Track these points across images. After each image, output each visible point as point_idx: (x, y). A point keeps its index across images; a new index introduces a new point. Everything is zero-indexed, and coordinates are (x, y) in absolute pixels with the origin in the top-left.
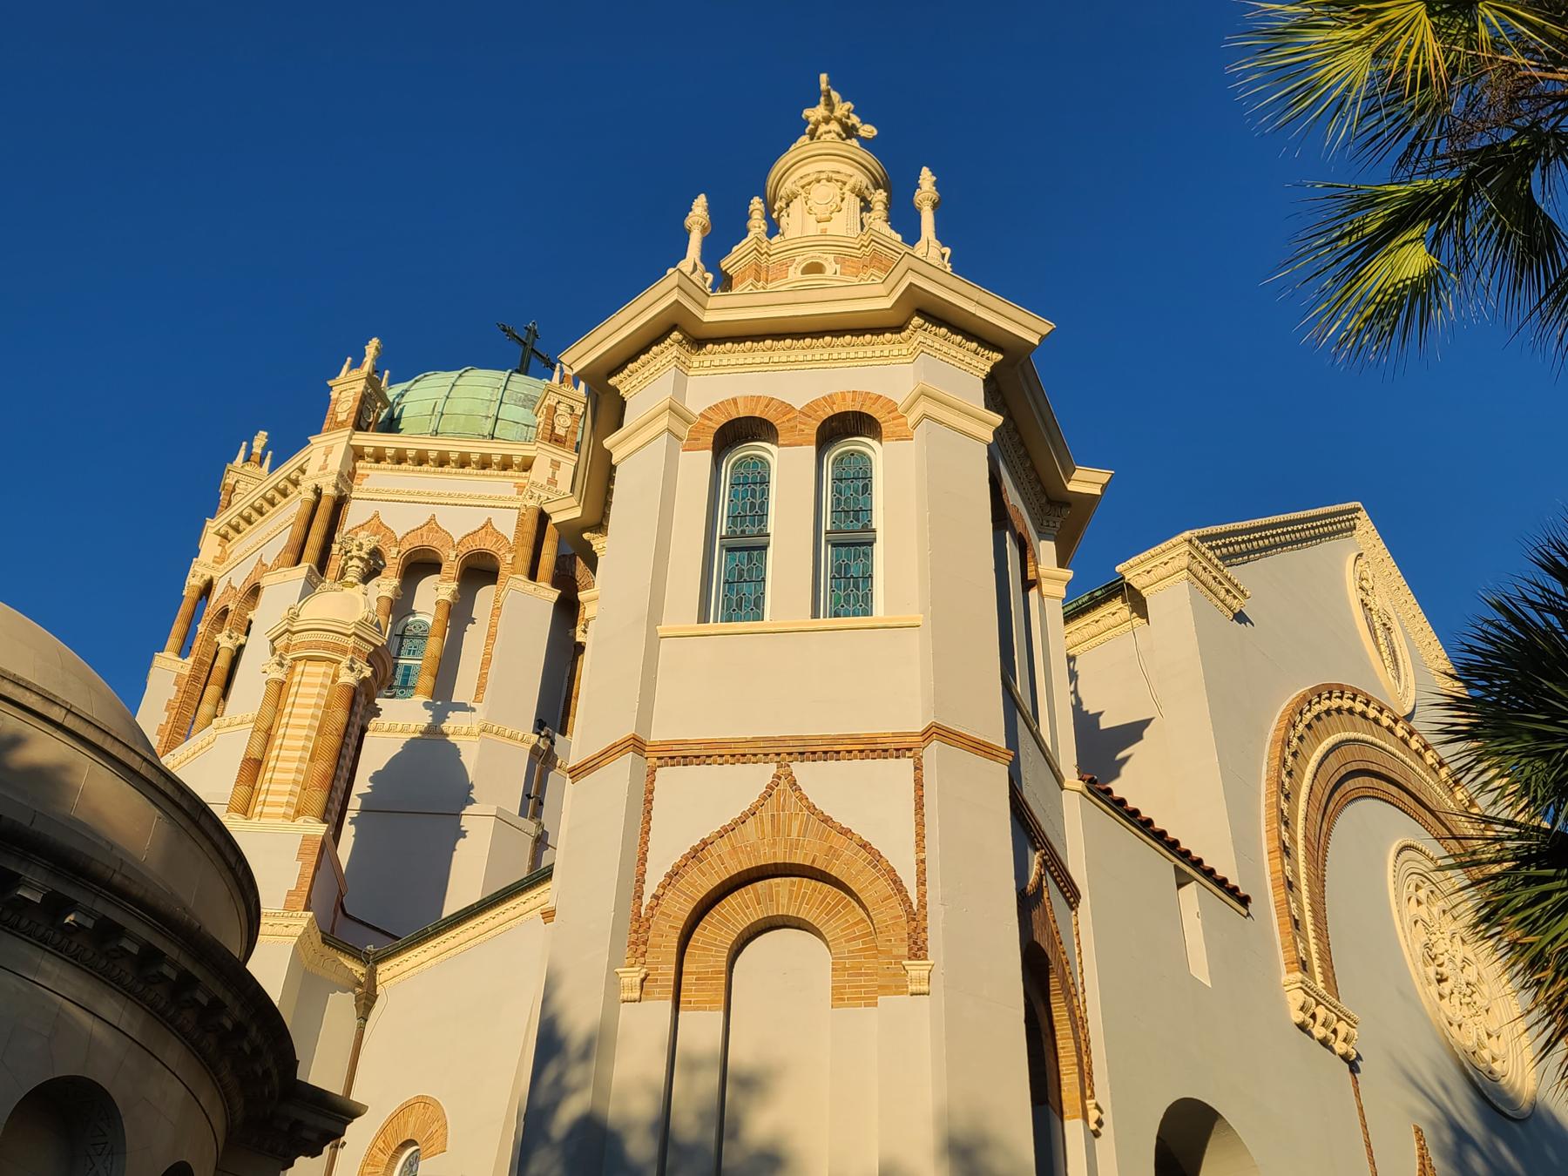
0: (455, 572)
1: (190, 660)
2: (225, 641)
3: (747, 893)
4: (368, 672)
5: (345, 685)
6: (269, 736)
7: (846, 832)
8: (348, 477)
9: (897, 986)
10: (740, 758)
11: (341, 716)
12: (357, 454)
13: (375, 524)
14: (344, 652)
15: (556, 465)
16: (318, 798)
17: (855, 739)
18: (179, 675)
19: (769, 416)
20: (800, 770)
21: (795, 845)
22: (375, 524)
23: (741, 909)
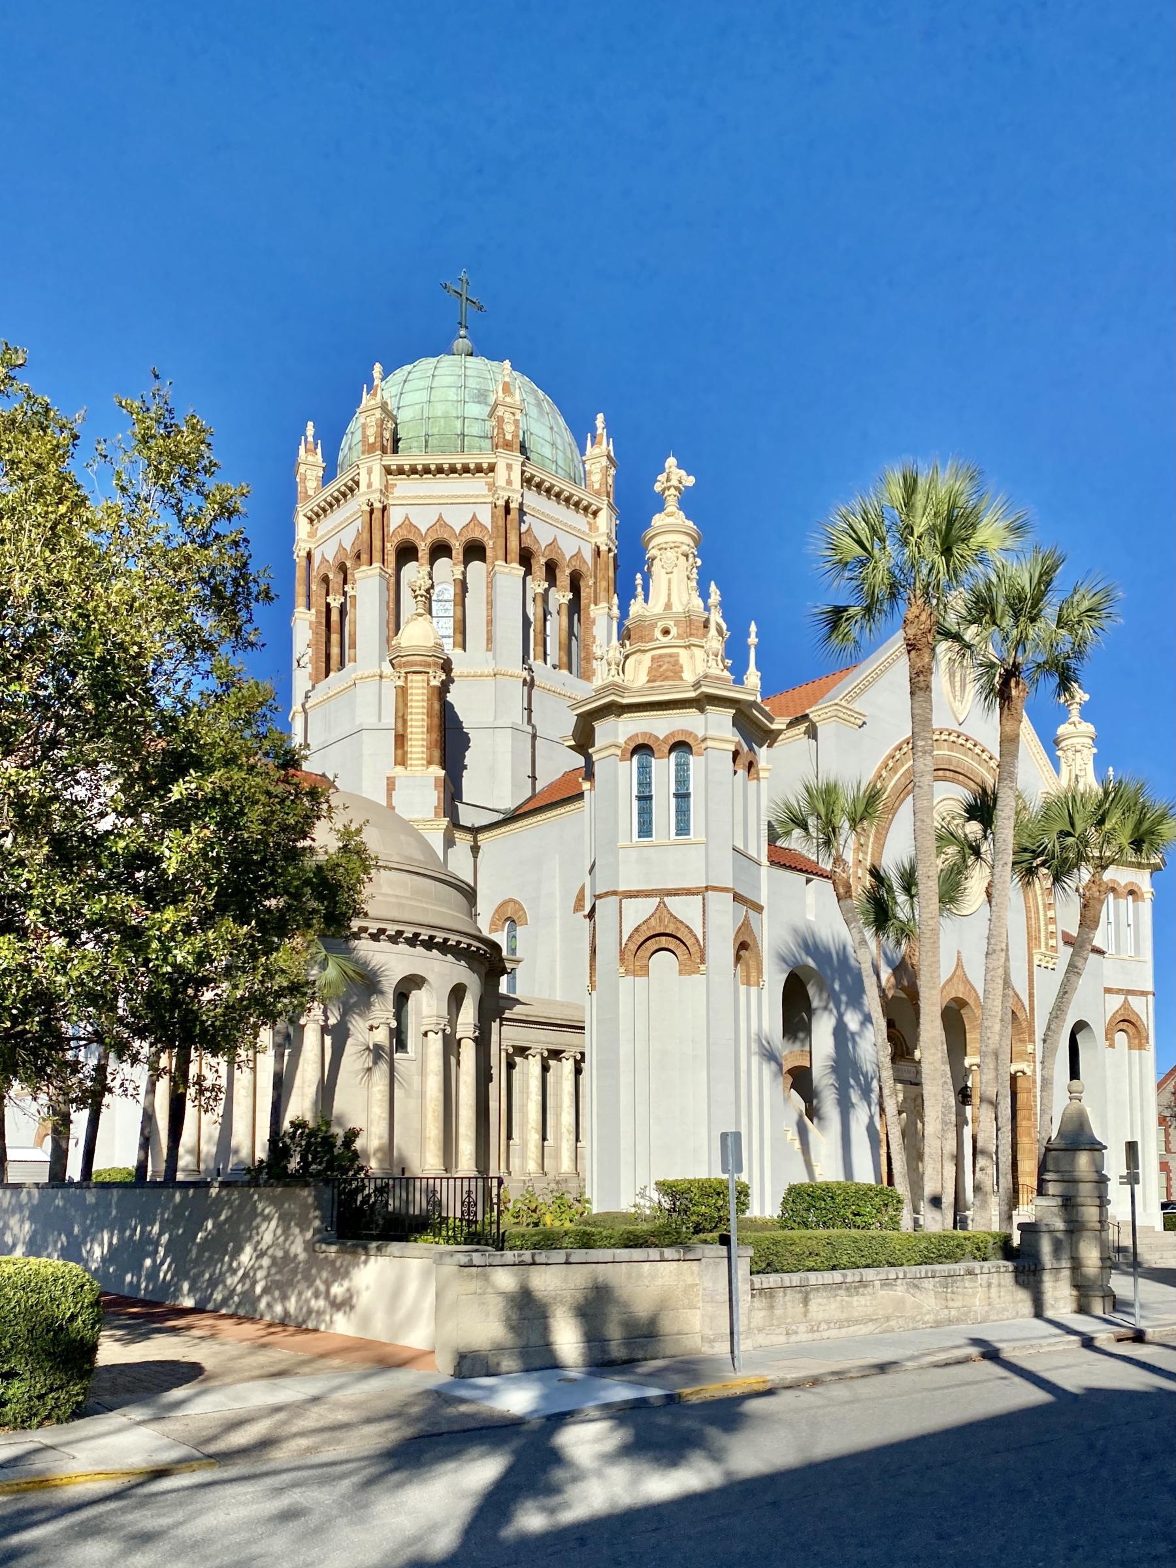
0: (461, 557)
1: (313, 611)
2: (335, 602)
4: (444, 677)
5: (434, 687)
6: (405, 721)
8: (386, 490)
9: (698, 972)
11: (437, 706)
12: (388, 471)
13: (407, 524)
14: (429, 665)
16: (437, 754)
18: (311, 622)
19: (650, 743)
22: (407, 524)
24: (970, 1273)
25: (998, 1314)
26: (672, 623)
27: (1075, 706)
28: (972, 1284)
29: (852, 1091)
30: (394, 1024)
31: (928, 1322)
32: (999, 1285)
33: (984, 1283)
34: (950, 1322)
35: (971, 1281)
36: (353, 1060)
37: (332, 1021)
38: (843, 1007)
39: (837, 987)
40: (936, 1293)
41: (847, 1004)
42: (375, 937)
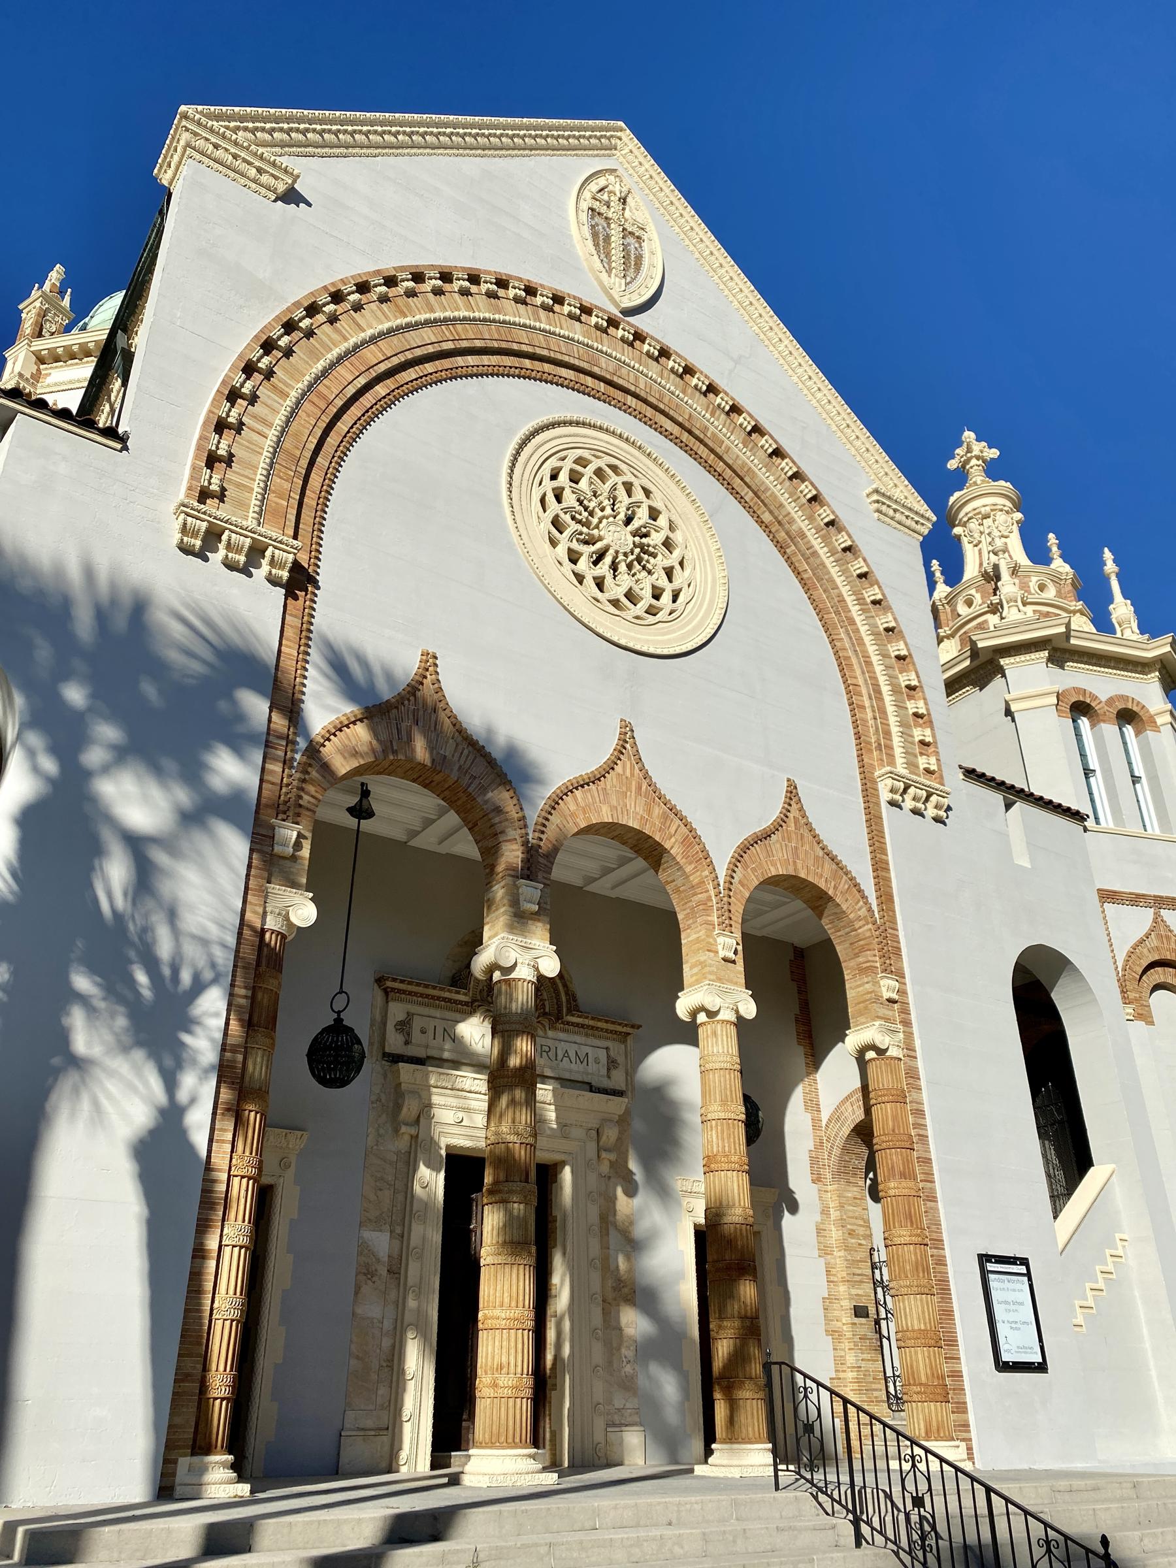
27: (974, 462)
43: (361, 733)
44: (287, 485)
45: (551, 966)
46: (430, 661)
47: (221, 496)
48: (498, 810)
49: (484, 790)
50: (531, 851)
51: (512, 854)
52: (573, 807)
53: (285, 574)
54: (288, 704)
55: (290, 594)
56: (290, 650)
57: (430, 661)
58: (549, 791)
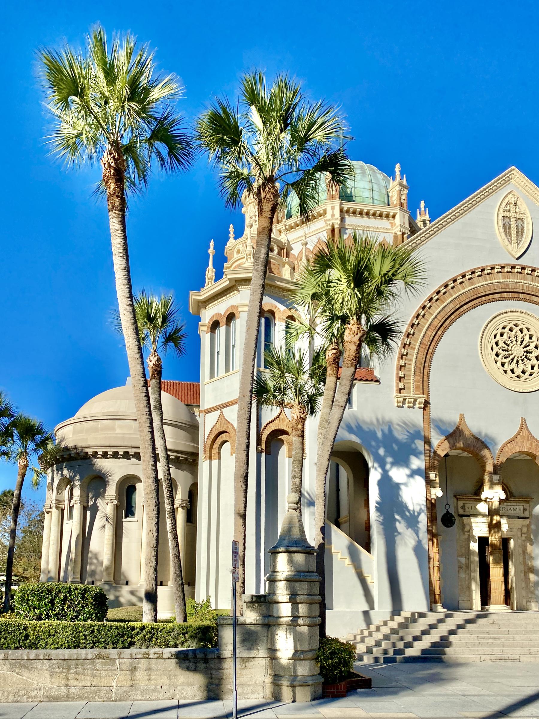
3: (220, 436)
7: (229, 422)
10: (215, 410)
15: (333, 208)
17: (230, 402)
20: (224, 410)
21: (223, 427)
23: (219, 440)
24: (100, 657)
25: (143, 693)
26: (241, 246)
28: (106, 667)
29: (397, 523)
30: (115, 502)
31: (36, 697)
32: (149, 670)
33: (125, 667)
34: (68, 697)
35: (103, 664)
36: (98, 523)
37: (91, 503)
38: (388, 466)
39: (381, 452)
40: (52, 674)
41: (393, 464)
42: (105, 455)
43: (446, 444)
44: (419, 378)
45: (503, 496)
46: (462, 416)
47: (404, 389)
48: (485, 456)
49: (481, 450)
50: (495, 467)
51: (489, 468)
52: (507, 450)
53: (422, 406)
54: (428, 442)
55: (424, 409)
56: (426, 426)
57: (462, 416)
58: (499, 447)
